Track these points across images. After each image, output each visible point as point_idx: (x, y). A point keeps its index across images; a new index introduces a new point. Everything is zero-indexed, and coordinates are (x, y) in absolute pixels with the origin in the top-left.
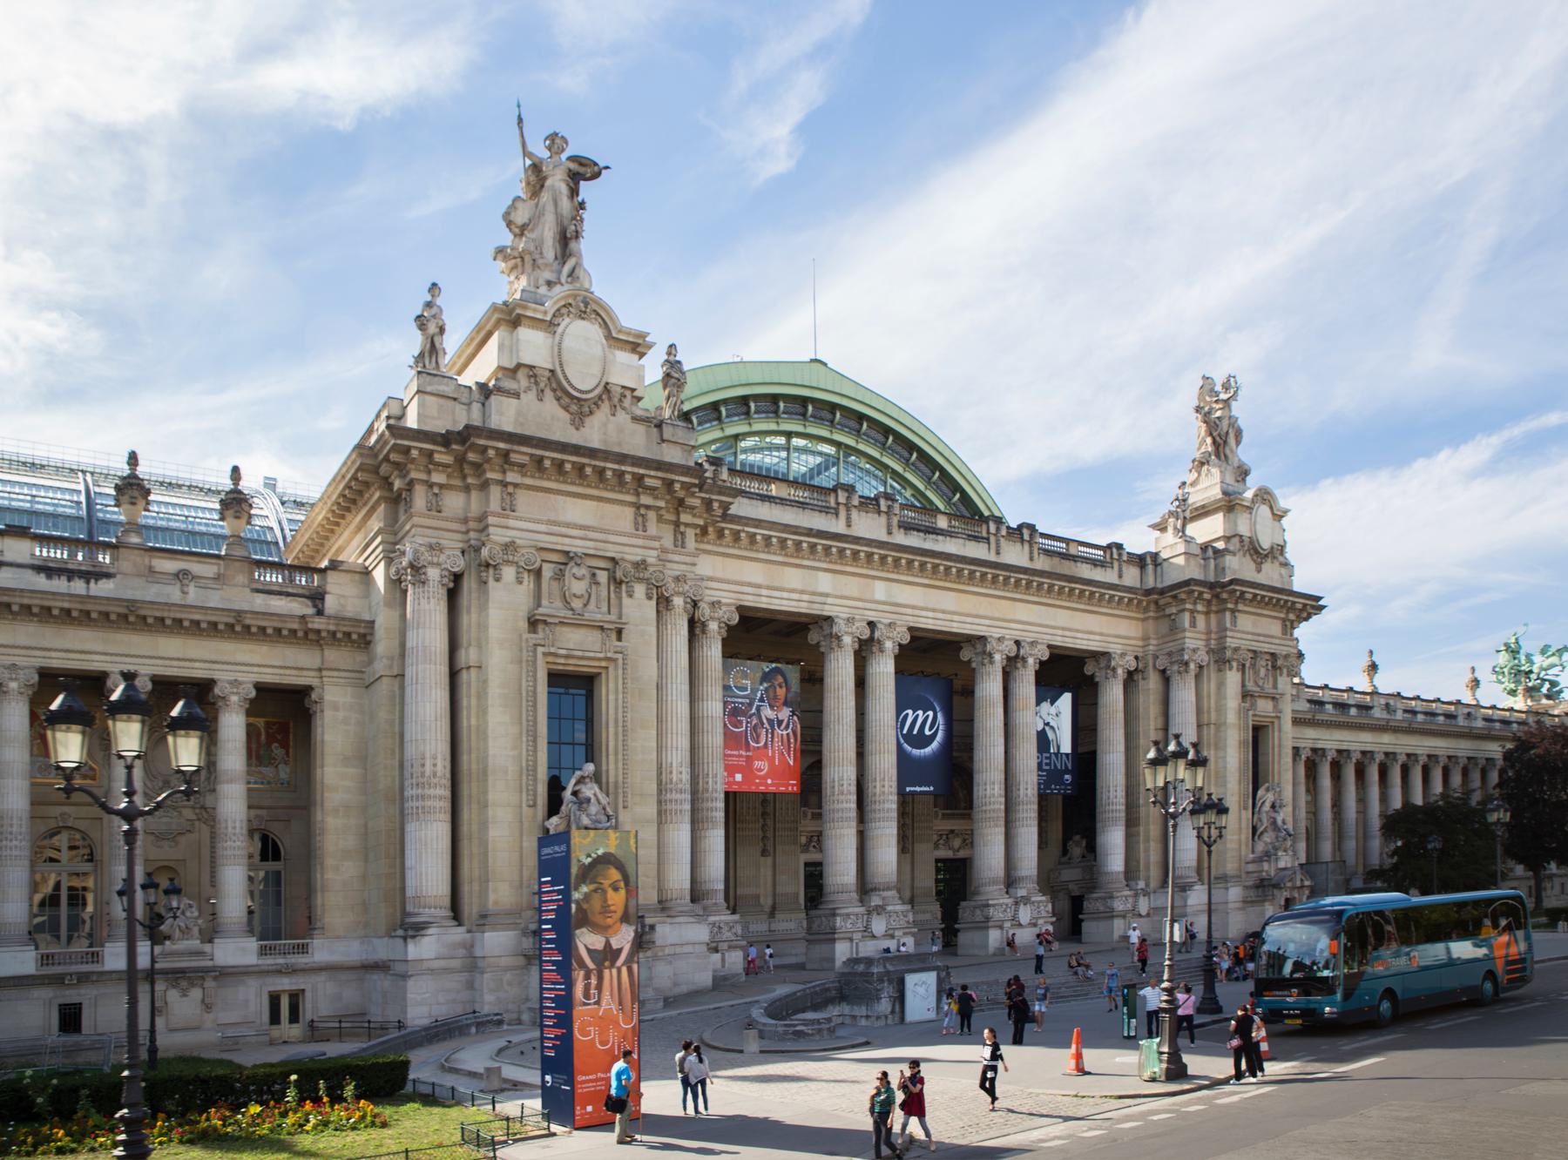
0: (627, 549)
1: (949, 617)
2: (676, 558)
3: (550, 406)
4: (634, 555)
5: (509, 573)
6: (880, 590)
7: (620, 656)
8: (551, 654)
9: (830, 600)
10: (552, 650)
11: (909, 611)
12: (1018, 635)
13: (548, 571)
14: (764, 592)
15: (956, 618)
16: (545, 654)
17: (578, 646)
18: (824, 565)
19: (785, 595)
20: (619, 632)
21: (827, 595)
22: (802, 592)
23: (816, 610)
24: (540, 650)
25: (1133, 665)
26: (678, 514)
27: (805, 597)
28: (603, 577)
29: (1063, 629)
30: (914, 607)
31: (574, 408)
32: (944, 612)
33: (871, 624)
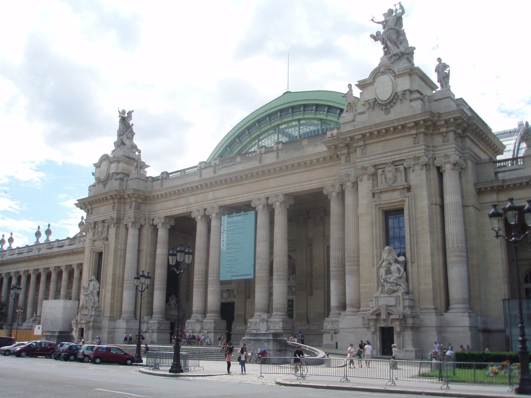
0: (417, 152)
2: (443, 148)
3: (377, 110)
4: (412, 155)
5: (365, 177)
7: (407, 199)
8: (379, 204)
10: (377, 203)
13: (380, 172)
16: (376, 205)
17: (392, 199)
20: (409, 189)
24: (374, 204)
26: (439, 129)
28: (401, 168)
31: (384, 108)
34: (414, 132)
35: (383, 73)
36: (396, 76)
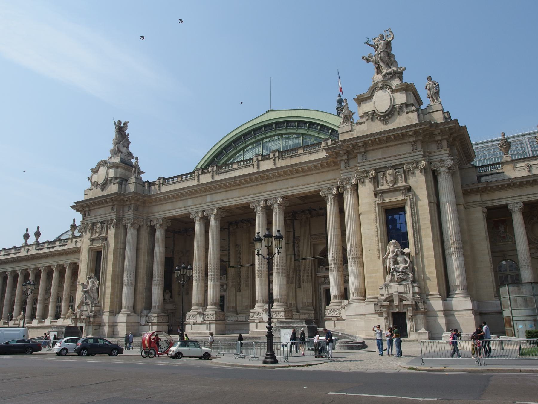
1: (235, 199)
6: (208, 199)
9: (190, 208)
11: (219, 202)
12: (266, 197)
14: (171, 211)
15: (238, 199)
18: (187, 197)
19: (177, 210)
21: (189, 206)
22: (181, 208)
23: (187, 212)
25: (335, 191)
27: (183, 209)
28: (105, 225)
29: (291, 187)
30: (219, 201)
32: (232, 198)
33: (203, 211)
34: (111, 204)
35: (103, 165)
36: (109, 168)
